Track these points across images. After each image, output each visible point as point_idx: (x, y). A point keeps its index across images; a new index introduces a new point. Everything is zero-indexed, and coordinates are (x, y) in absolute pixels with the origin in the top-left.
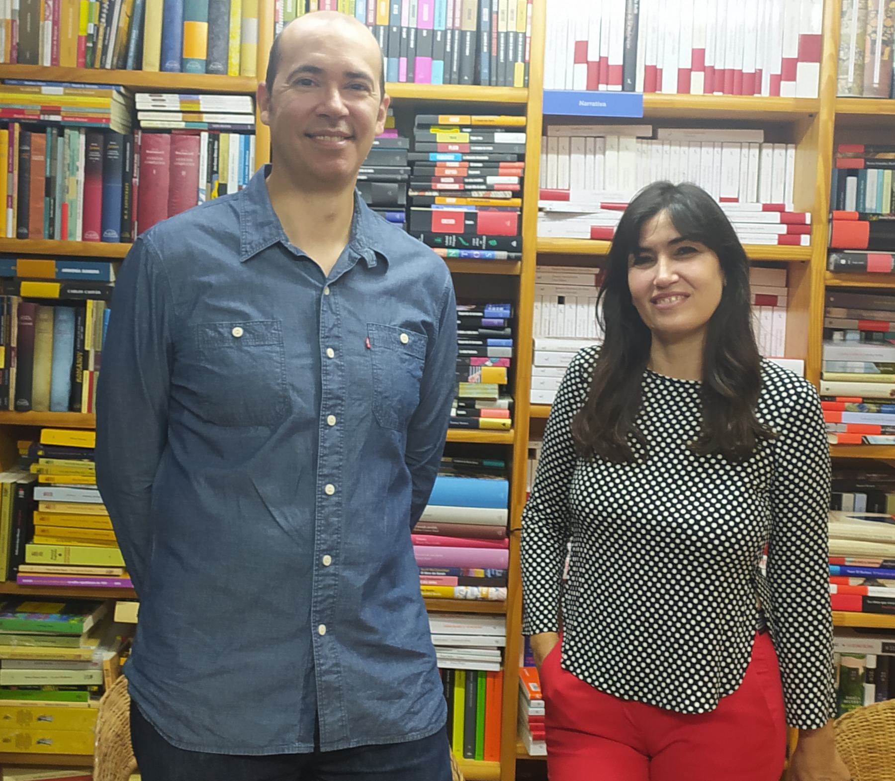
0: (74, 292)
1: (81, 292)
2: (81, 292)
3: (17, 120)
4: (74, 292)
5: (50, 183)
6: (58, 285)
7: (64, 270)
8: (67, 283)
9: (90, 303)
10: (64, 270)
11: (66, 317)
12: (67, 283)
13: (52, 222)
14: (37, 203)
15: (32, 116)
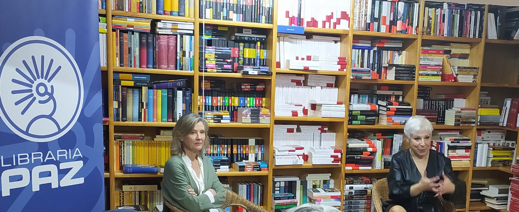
0: (139, 84)
1: (141, 84)
2: (141, 84)
3: (119, 29)
4: (139, 84)
5: (130, 49)
6: (133, 82)
7: (135, 77)
8: (136, 81)
9: (143, 87)
10: (135, 77)
11: (137, 92)
12: (136, 81)
13: (131, 61)
14: (126, 56)
15: (122, 28)
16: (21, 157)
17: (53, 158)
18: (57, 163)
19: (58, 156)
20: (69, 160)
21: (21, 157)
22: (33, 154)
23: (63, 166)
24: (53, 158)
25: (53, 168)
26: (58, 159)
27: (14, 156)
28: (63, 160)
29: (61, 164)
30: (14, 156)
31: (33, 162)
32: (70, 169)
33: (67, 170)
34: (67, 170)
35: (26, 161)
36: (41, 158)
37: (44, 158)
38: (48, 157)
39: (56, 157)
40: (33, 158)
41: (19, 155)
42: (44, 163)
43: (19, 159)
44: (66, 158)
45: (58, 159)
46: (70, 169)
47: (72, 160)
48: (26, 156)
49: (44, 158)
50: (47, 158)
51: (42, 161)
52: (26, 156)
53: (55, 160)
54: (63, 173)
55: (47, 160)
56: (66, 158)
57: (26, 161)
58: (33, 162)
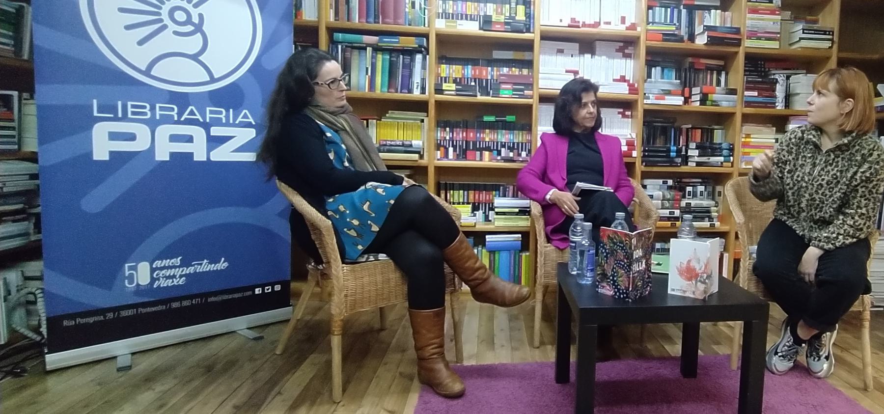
16: (133, 106)
17: (199, 117)
18: (206, 126)
19: (208, 115)
20: (227, 124)
21: (133, 106)
22: (158, 105)
23: (215, 131)
24: (199, 117)
25: (198, 133)
26: (208, 120)
27: (120, 104)
28: (217, 122)
29: (212, 129)
30: (120, 104)
31: (158, 117)
32: (230, 138)
33: (224, 140)
34: (224, 140)
35: (145, 114)
36: (174, 113)
37: (180, 114)
38: (188, 115)
39: (204, 117)
40: (158, 112)
41: (129, 104)
42: (178, 122)
43: (130, 110)
44: (224, 121)
45: (208, 120)
46: (230, 138)
47: (234, 125)
48: (144, 107)
49: (180, 114)
50: (185, 116)
51: (176, 119)
52: (144, 107)
53: (201, 120)
54: (215, 142)
55: (186, 119)
56: (224, 121)
57: (145, 114)
58: (158, 117)
